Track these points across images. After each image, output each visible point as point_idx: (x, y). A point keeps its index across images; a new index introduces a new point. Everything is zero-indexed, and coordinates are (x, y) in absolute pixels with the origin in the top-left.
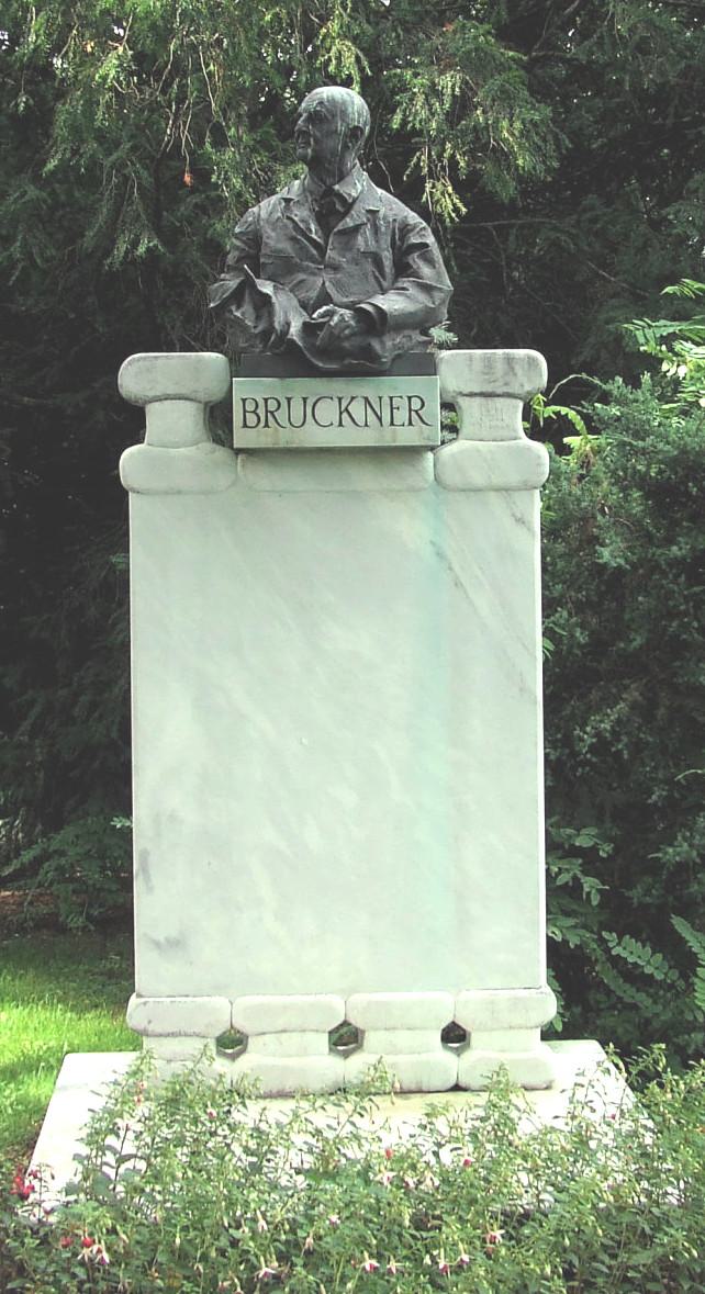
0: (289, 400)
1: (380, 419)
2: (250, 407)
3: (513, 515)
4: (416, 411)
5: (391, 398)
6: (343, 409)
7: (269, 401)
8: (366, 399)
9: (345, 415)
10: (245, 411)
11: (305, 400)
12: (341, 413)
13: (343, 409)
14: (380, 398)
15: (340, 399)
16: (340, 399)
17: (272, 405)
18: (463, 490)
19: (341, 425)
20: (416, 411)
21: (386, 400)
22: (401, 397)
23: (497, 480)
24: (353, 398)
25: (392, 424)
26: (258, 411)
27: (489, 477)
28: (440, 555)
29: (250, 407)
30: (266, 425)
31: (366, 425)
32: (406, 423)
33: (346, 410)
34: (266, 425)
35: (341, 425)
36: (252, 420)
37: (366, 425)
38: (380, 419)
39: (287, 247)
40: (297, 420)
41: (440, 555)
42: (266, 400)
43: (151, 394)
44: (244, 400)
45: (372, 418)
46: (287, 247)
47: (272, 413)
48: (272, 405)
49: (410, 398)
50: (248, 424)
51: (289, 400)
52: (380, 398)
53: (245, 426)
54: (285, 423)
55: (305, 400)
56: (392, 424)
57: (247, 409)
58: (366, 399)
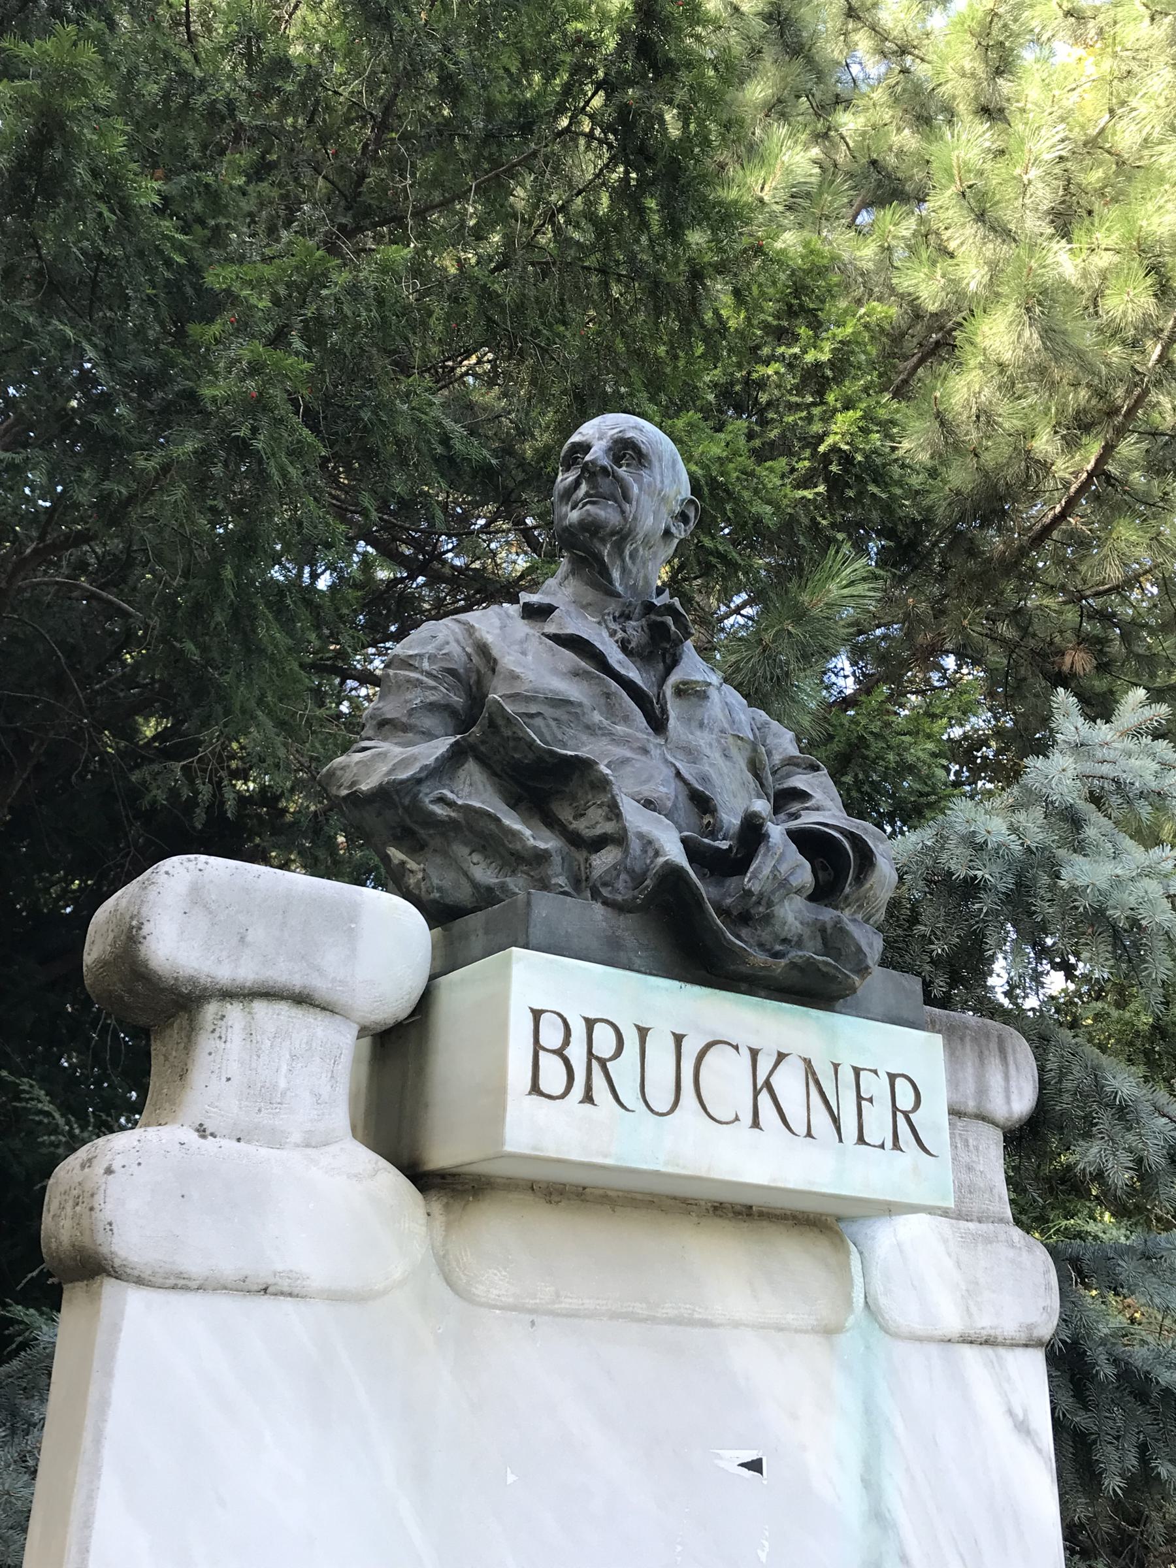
0: (643, 1032)
1: (836, 1121)
2: (551, 1036)
3: (1011, 1413)
4: (904, 1113)
5: (857, 1071)
6: (760, 1083)
7: (598, 1027)
8: (808, 1063)
9: (764, 1098)
10: (537, 1046)
11: (679, 1039)
12: (756, 1093)
13: (760, 1082)
14: (836, 1067)
15: (754, 1053)
16: (754, 1053)
17: (604, 1042)
18: (920, 1339)
19: (756, 1124)
20: (906, 1115)
21: (847, 1075)
22: (875, 1072)
23: (985, 1323)
24: (781, 1057)
25: (861, 1140)
26: (569, 1052)
27: (970, 1315)
28: (878, 1516)
29: (551, 1036)
30: (588, 1098)
31: (809, 1134)
32: (889, 1144)
33: (768, 1084)
34: (588, 1098)
35: (756, 1124)
36: (553, 1074)
37: (809, 1134)
38: (836, 1121)
39: (573, 690)
40: (661, 1097)
41: (878, 1516)
42: (590, 1024)
43: (225, 972)
44: (537, 1014)
45: (821, 1119)
46: (573, 690)
47: (603, 1063)
48: (604, 1042)
49: (892, 1078)
50: (544, 1086)
51: (643, 1032)
52: (836, 1067)
53: (535, 1089)
54: (628, 1092)
55: (679, 1039)
56: (861, 1140)
57: (542, 1042)
58: (808, 1063)
